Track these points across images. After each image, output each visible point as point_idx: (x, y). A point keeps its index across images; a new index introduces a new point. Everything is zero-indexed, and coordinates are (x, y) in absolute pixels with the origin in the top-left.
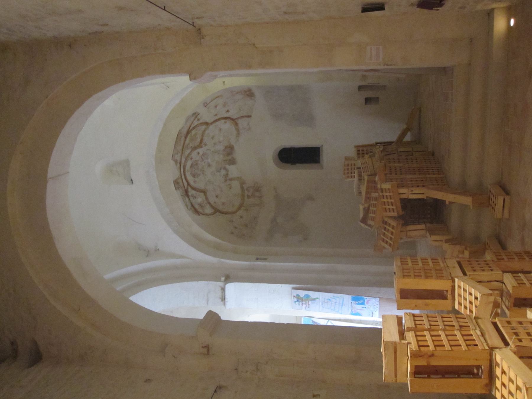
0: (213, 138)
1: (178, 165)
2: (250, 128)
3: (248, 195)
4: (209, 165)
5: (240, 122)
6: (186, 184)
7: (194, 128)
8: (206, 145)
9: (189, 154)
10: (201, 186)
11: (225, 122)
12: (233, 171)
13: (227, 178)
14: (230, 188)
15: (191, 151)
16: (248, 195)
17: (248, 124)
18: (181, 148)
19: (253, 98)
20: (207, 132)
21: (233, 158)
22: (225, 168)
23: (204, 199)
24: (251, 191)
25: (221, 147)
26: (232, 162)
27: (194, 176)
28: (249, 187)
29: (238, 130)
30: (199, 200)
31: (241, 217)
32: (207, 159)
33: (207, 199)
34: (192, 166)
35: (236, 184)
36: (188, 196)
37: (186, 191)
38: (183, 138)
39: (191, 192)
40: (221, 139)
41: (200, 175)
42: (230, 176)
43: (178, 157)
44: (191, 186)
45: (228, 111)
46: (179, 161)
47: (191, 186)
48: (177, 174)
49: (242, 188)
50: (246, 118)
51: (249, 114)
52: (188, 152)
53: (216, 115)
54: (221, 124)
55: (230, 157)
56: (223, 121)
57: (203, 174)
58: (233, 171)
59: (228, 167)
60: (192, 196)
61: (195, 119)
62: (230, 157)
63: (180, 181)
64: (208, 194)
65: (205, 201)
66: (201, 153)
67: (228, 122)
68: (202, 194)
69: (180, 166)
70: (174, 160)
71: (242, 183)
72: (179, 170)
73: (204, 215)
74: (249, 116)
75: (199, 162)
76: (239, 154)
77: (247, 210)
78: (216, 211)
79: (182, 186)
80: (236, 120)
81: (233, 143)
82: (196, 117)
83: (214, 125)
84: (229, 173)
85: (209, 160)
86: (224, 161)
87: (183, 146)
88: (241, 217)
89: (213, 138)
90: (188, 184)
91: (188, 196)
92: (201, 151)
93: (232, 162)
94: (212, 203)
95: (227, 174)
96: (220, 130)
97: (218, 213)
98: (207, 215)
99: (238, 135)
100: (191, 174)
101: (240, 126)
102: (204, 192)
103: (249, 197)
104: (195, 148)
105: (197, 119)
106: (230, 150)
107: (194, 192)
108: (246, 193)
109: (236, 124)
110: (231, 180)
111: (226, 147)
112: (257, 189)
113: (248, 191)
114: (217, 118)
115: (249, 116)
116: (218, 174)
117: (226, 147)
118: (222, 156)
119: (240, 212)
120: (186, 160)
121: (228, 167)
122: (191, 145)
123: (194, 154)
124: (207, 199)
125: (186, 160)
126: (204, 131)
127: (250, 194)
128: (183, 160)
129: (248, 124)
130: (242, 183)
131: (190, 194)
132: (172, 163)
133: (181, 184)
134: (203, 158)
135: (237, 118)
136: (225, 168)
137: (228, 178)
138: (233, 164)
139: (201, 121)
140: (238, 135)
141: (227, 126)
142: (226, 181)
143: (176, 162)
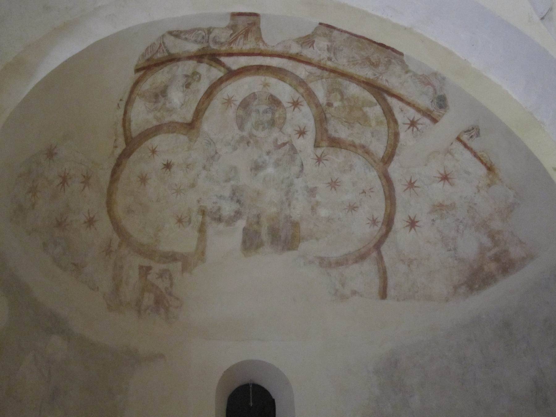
0: (334, 184)
1: (295, 49)
2: (343, 298)
3: (149, 268)
4: (257, 167)
5: (369, 267)
6: (235, 63)
7: (388, 112)
8: (319, 160)
9: (310, 95)
10: (208, 126)
11: (374, 222)
12: (226, 241)
13: (209, 216)
14: (180, 221)
15: (318, 105)
16: (149, 268)
17: (354, 293)
18: (342, 62)
19: (463, 289)
20: (358, 162)
21: (261, 245)
22: (238, 214)
23: (176, 118)
24: (162, 284)
25: (299, 209)
26: (251, 242)
27: (245, 104)
28: (171, 278)
29: (339, 263)
30: (176, 97)
31: (90, 222)
32: (277, 164)
33: (173, 127)
34: (274, 102)
35: (182, 241)
36: (199, 57)
37: (210, 56)
38: (367, 73)
39: (209, 73)
40: (323, 212)
41: (241, 127)
42: (212, 229)
43: (318, 51)
44: (221, 81)
45: (413, 224)
46: (308, 53)
47: (221, 81)
48: (272, 38)
49: (173, 257)
50: (376, 282)
51: (391, 292)
52: (320, 91)
53: (411, 185)
54: (377, 205)
55: (265, 236)
56: (380, 215)
57: (242, 138)
58: (226, 241)
59: (241, 224)
60: (195, 73)
61: (418, 110)
62: (265, 236)
63: (249, 46)
64: (183, 138)
65: (167, 119)
66: (299, 143)
67: (376, 231)
68: (189, 117)
69: (291, 58)
70: (314, 34)
71: (186, 262)
72: (279, 49)
73: (132, 92)
74: (383, 295)
75: (275, 134)
76: (272, 264)
77: (108, 251)
78: (132, 143)
79: (235, 48)
80: (374, 254)
81: (303, 246)
82: (427, 113)
83: (378, 185)
84: (221, 226)
85: (270, 170)
86: (258, 216)
87: (343, 75)
88: (90, 222)
89: (334, 184)
90: (232, 74)
91: (199, 57)
92: (305, 145)
93: (251, 242)
94: (157, 141)
95: (219, 220)
96: (353, 208)
97: (122, 146)
98: (129, 102)
99: (326, 264)
100: (254, 96)
101: (353, 270)
102: (191, 126)
103: (145, 271)
104: (321, 120)
105: (418, 116)
106: (286, 236)
107: (203, 86)
108: (157, 267)
109: (361, 257)
110: (202, 230)
111: (295, 225)
112: (162, 303)
113: (162, 275)
114: (399, 188)
115: (383, 295)
116: (227, 193)
117: (295, 225)
118: (274, 210)
119: (104, 225)
120: (300, 83)
121: (241, 224)
122: (336, 104)
123: (305, 116)
124: (173, 127)
125: (300, 83)
126: (366, 151)
127: (151, 277)
128: (302, 71)
129: (354, 293)
130: (186, 262)
131: (203, 68)
132: (310, 21)
133: (241, 45)
134: (282, 151)
135: (380, 258)
136: (238, 214)
137: (208, 219)
138: (244, 242)
139: (405, 135)
140: (326, 264)
141: (361, 229)
142: (203, 212)
143: (307, 41)
